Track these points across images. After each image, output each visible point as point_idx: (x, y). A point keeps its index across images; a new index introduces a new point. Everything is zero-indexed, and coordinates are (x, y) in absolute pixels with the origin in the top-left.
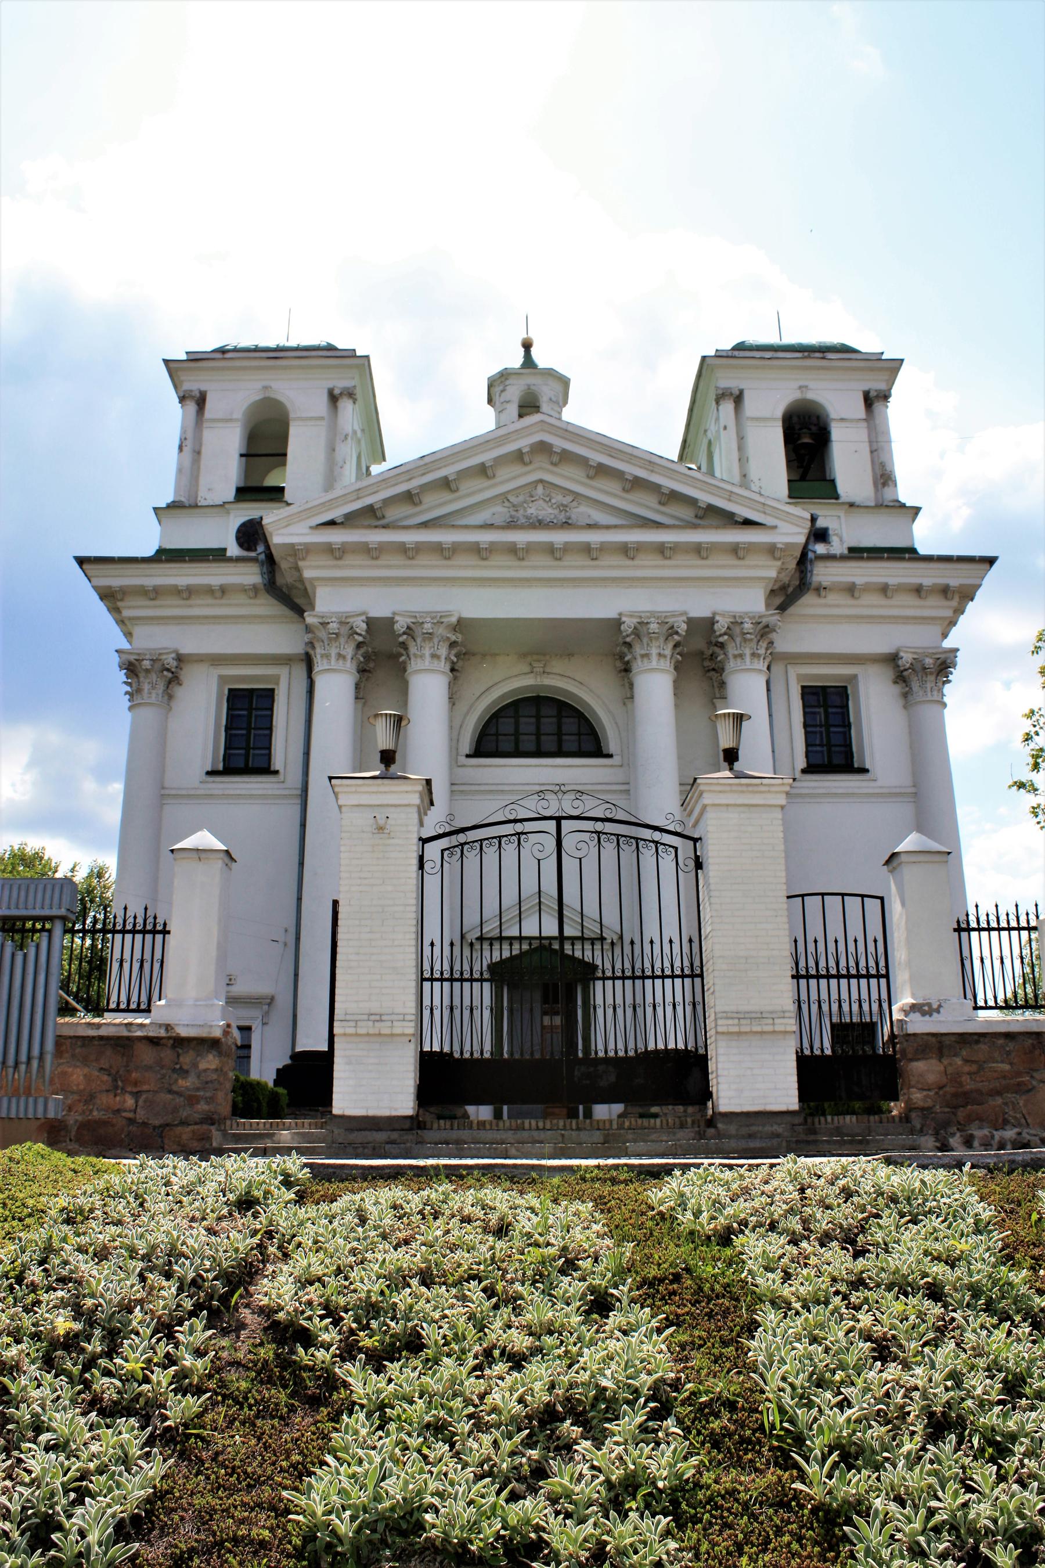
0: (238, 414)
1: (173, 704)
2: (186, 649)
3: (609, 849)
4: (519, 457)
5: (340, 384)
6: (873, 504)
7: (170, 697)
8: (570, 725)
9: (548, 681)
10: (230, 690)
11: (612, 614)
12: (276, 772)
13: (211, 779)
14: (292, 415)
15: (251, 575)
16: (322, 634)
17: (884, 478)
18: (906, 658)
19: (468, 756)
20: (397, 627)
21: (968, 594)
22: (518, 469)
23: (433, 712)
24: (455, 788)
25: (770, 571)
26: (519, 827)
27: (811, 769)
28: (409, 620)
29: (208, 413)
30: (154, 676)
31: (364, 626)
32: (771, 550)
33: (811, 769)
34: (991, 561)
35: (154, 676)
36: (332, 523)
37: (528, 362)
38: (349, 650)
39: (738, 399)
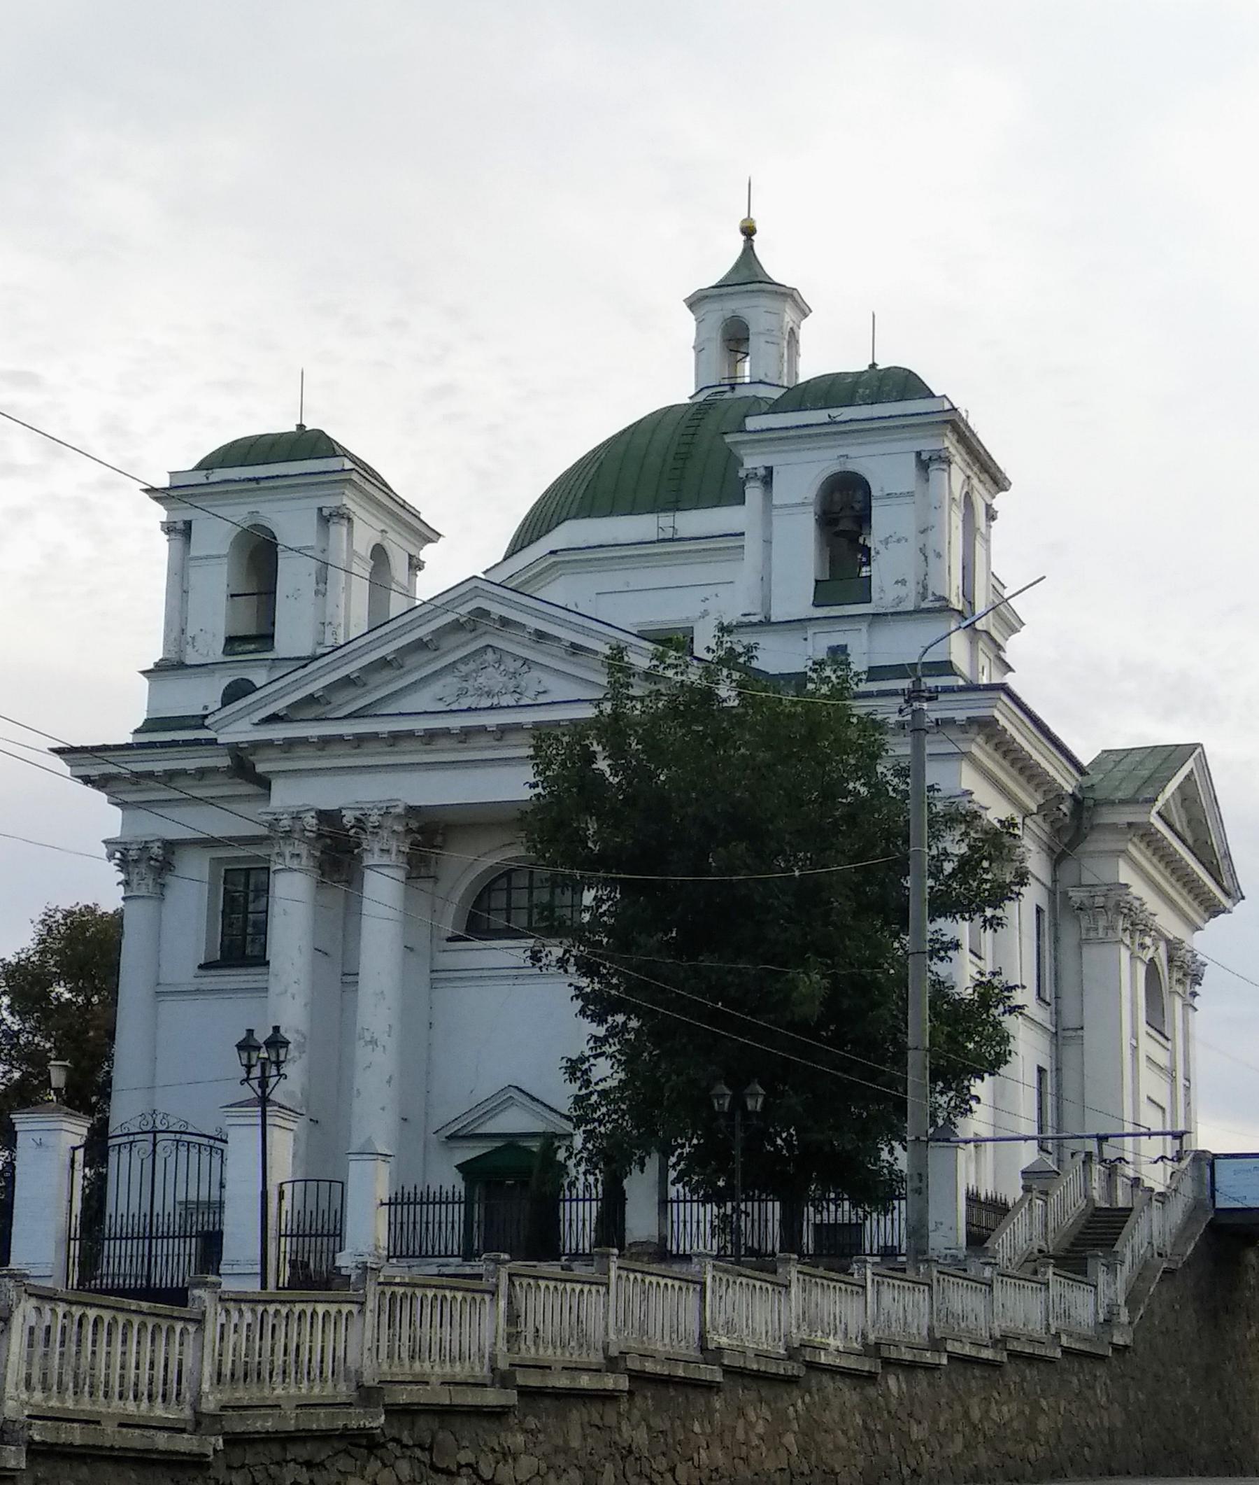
0: (225, 550)
1: (167, 892)
3: (183, 1149)
4: (457, 626)
5: (330, 503)
7: (163, 885)
10: (226, 871)
13: (203, 973)
19: (449, 940)
20: (345, 820)
22: (463, 637)
24: (435, 975)
26: (131, 1138)
28: (358, 813)
30: (143, 868)
31: (314, 821)
35: (143, 868)
36: (273, 719)
37: (748, 255)
38: (303, 849)
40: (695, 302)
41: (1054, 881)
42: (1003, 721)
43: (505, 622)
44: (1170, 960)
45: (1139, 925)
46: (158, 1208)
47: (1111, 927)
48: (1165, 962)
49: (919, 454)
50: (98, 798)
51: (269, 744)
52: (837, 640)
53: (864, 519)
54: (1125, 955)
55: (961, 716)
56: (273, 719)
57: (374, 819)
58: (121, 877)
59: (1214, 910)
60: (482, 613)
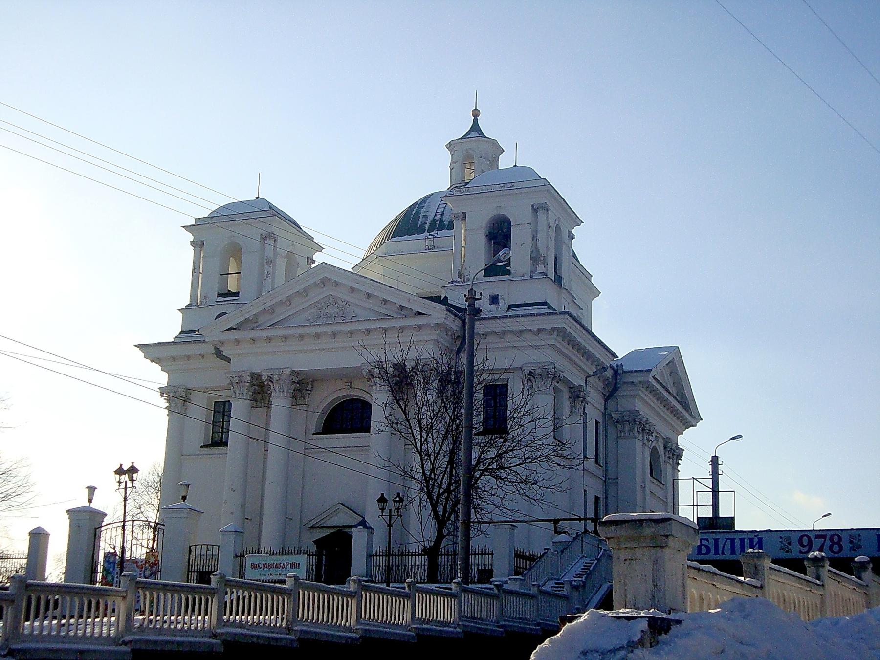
18: (527, 370)
32: (428, 325)
36: (231, 329)
40: (450, 146)
41: (605, 409)
42: (569, 330)
43: (337, 284)
44: (665, 448)
45: (645, 429)
47: (631, 430)
48: (662, 448)
49: (533, 206)
50: (157, 367)
54: (638, 444)
55: (549, 327)
56: (231, 329)
57: (276, 377)
58: (167, 404)
59: (688, 425)
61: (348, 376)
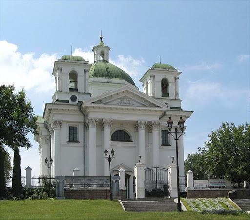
2: (64, 120)
6: (174, 99)
8: (126, 136)
9: (123, 128)
11: (136, 120)
12: (79, 142)
14: (78, 74)
15: (76, 108)
16: (91, 121)
17: (177, 94)
21: (189, 117)
23: (108, 133)
25: (160, 114)
27: (162, 145)
29: (63, 73)
32: (161, 111)
33: (162, 145)
34: (193, 112)
36: (94, 103)
39: (154, 77)
46: (158, 179)
51: (93, 107)
52: (166, 102)
53: (167, 85)
60: (127, 91)
61: (122, 123)
